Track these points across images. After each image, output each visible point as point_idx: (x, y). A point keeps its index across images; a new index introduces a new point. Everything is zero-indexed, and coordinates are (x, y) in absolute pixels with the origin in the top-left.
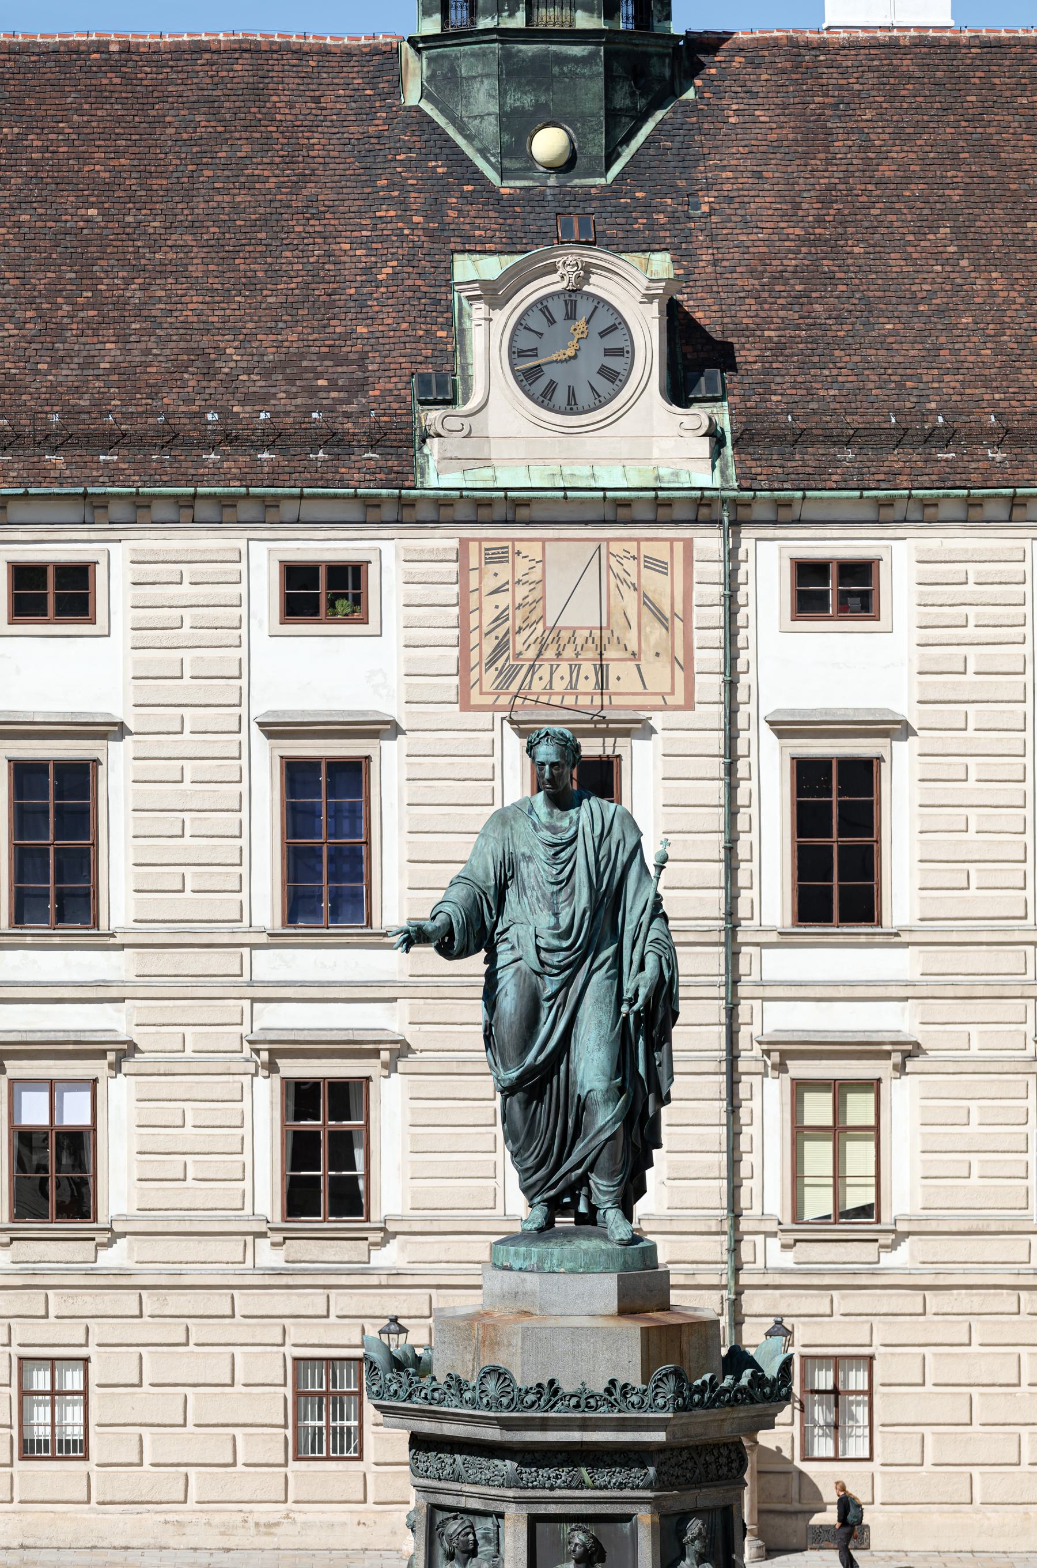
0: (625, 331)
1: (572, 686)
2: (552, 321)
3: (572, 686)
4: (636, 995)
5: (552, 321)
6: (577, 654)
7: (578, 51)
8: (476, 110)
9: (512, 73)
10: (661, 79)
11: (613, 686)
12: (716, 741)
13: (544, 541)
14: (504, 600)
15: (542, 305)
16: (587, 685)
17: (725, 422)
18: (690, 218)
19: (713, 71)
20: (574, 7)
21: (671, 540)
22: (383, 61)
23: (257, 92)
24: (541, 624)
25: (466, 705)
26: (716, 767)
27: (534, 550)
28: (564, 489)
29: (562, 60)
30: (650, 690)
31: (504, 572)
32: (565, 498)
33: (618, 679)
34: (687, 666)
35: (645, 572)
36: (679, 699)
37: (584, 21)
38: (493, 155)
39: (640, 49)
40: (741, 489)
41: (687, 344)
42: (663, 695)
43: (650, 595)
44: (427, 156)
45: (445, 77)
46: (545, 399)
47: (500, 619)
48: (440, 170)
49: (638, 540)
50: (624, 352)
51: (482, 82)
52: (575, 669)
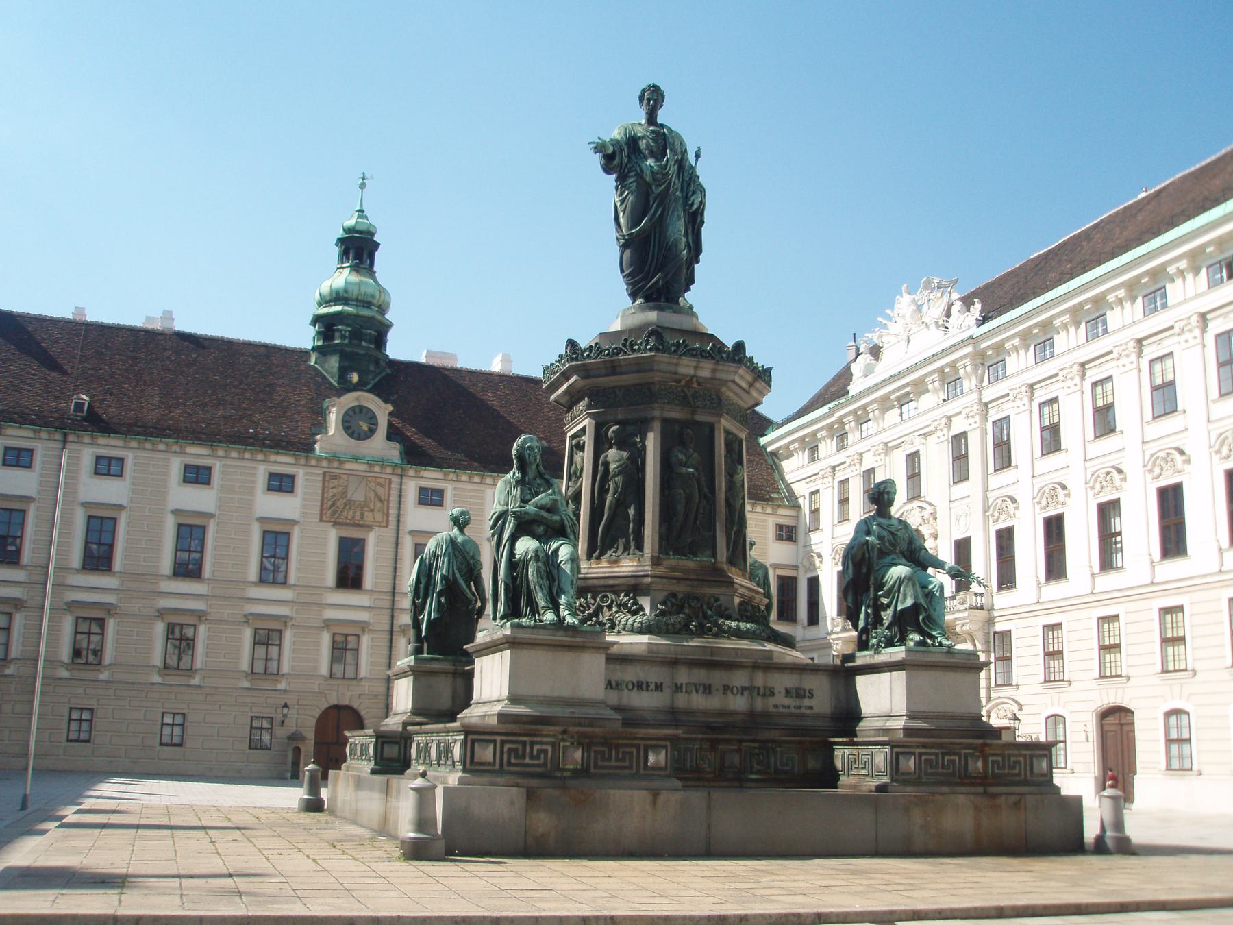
4: (692, 204)
9: (344, 356)
12: (393, 540)
14: (335, 490)
15: (353, 409)
16: (357, 518)
20: (361, 340)
22: (304, 354)
23: (267, 356)
25: (321, 520)
29: (357, 354)
31: (335, 482)
34: (388, 515)
46: (351, 435)
47: (334, 496)
50: (376, 424)
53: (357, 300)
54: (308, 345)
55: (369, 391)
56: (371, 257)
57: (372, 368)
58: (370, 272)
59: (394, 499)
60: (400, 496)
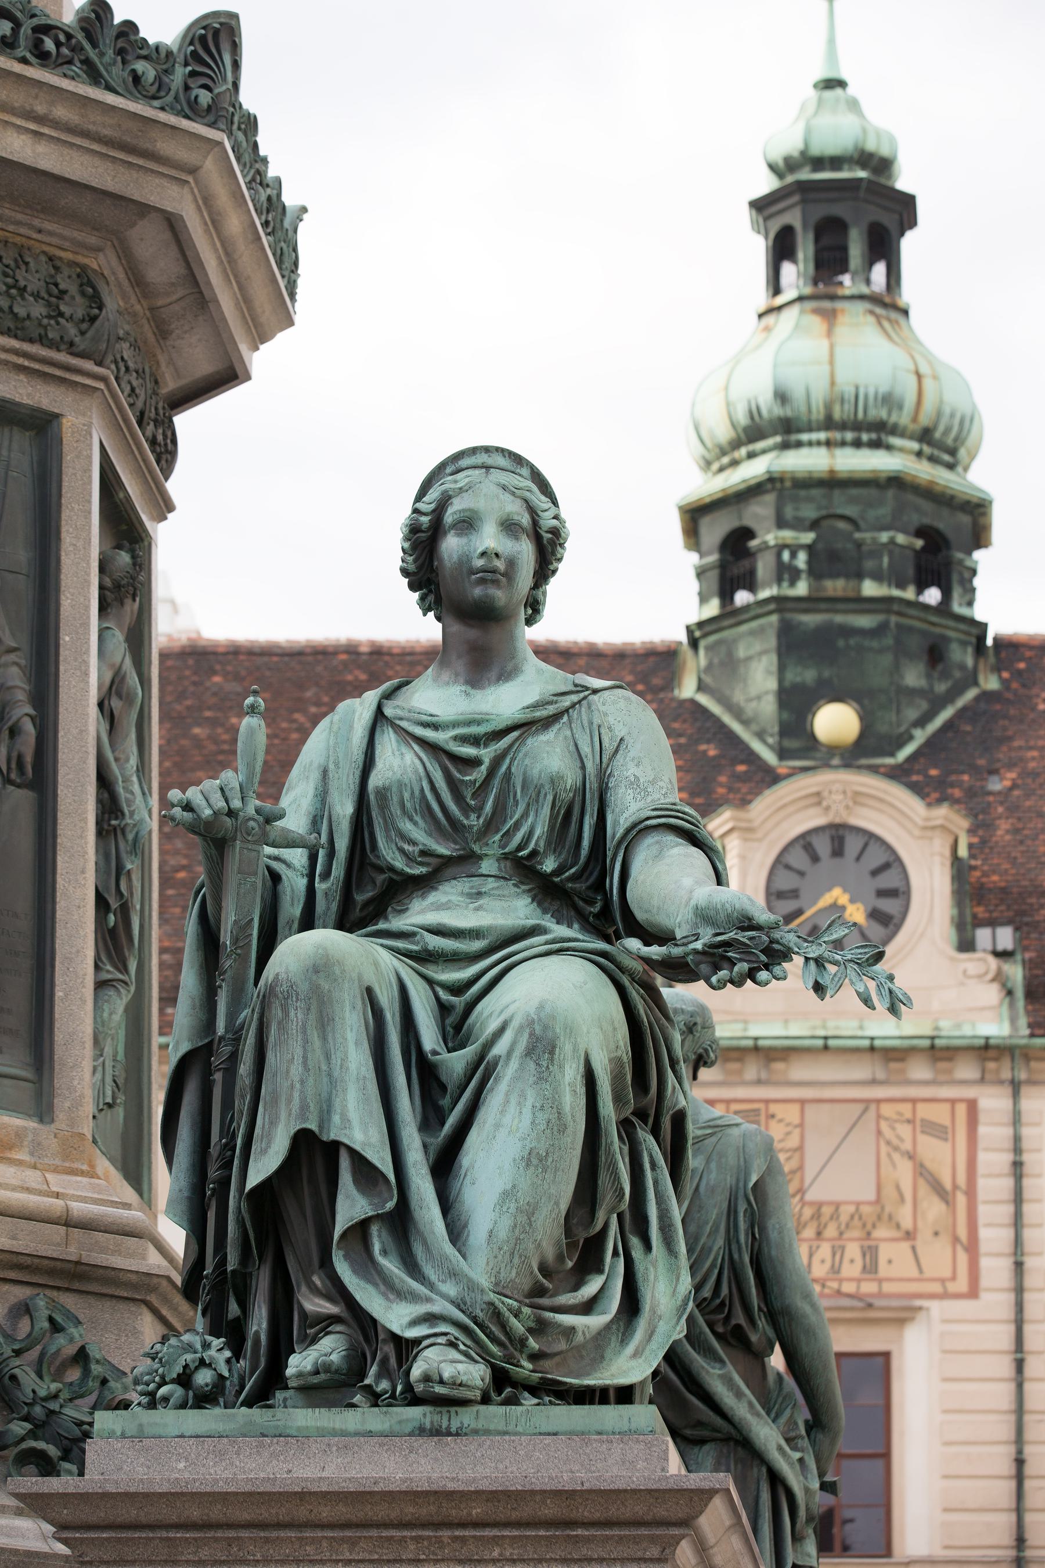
0: (900, 870)
1: (835, 1270)
2: (815, 858)
3: (835, 1270)
5: (815, 858)
6: (841, 1234)
7: (865, 621)
8: (753, 691)
9: (792, 645)
10: (962, 667)
11: (883, 1270)
13: (803, 1102)
15: (805, 841)
16: (852, 1269)
17: (1016, 972)
18: (990, 793)
19: (1022, 665)
21: (953, 1102)
24: (798, 1198)
26: (1005, 1367)
27: (791, 1113)
28: (826, 1038)
29: (848, 631)
30: (927, 1274)
32: (826, 1048)
33: (890, 1262)
34: (972, 1247)
35: (922, 1138)
36: (962, 1284)
37: (870, 588)
38: (772, 735)
39: (937, 630)
40: (1032, 1035)
41: (979, 904)
42: (943, 1281)
43: (928, 1164)
44: (698, 742)
45: (722, 664)
48: (712, 753)
49: (914, 1101)
50: (900, 893)
51: (760, 660)
52: (838, 1251)
53: (829, 423)
54: (672, 631)
55: (897, 774)
56: (884, 246)
57: (913, 677)
58: (889, 306)
59: (993, 1185)
60: (1017, 1168)
